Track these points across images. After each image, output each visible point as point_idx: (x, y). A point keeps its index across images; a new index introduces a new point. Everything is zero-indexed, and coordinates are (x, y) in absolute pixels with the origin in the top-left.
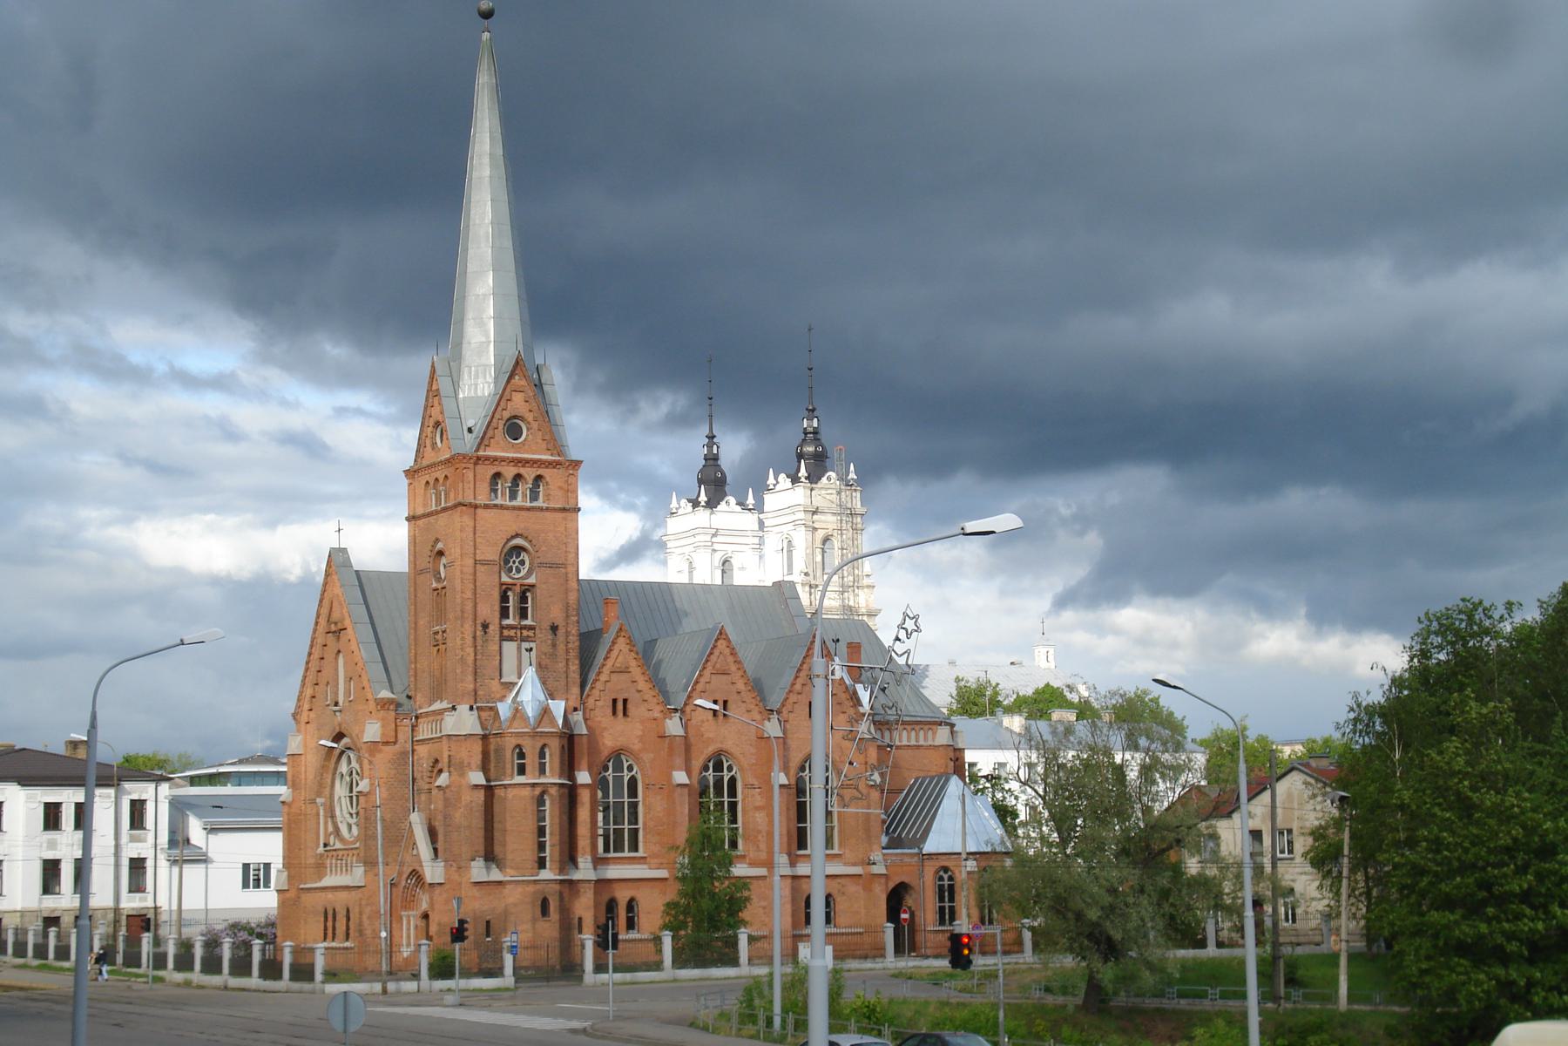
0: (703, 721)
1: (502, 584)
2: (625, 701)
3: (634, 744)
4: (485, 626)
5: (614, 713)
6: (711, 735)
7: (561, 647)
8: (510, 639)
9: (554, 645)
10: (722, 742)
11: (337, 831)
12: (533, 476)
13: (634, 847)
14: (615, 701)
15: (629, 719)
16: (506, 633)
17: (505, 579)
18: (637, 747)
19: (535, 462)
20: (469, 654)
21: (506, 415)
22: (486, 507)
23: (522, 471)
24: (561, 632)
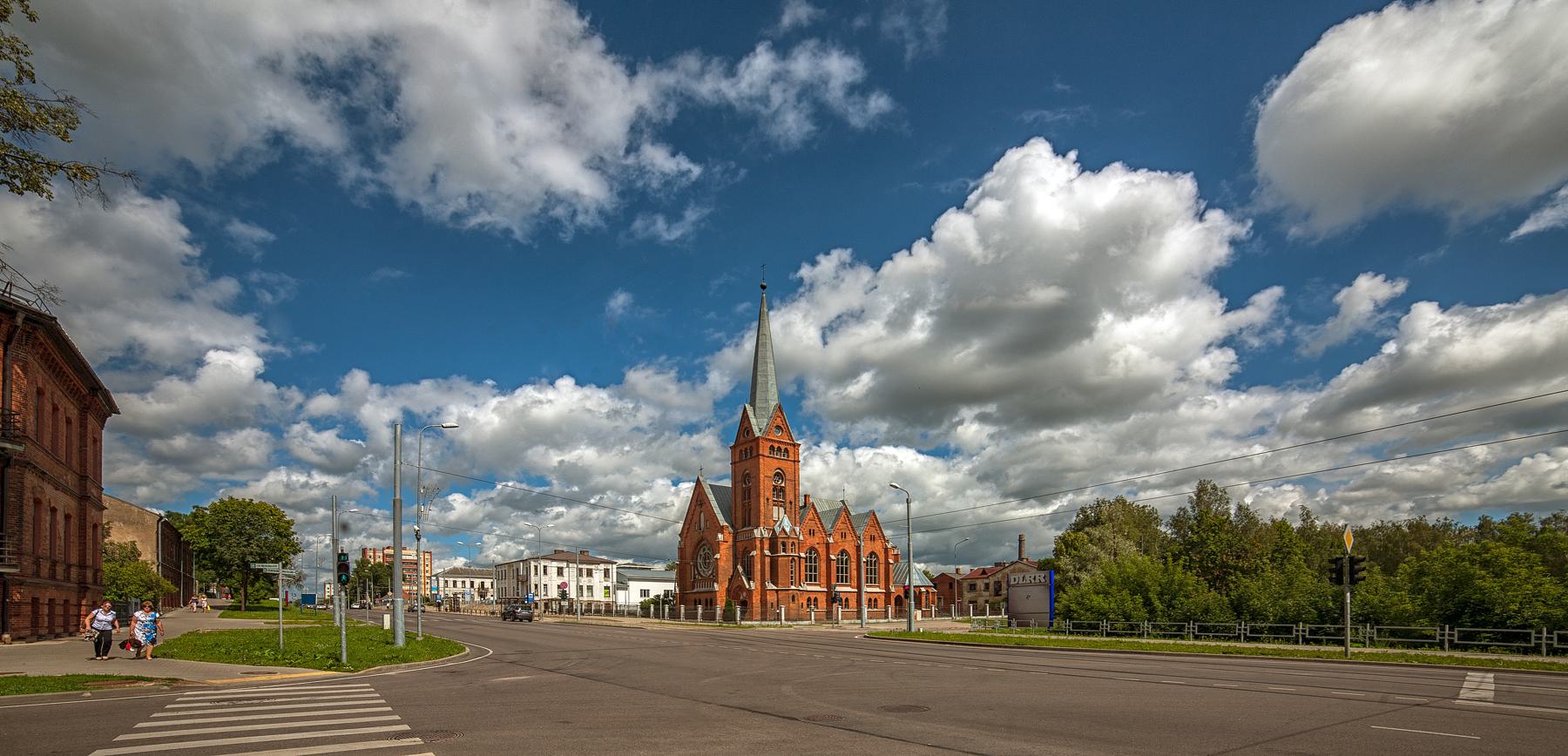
4: (768, 499)
11: (699, 574)
21: (775, 425)
22: (768, 457)
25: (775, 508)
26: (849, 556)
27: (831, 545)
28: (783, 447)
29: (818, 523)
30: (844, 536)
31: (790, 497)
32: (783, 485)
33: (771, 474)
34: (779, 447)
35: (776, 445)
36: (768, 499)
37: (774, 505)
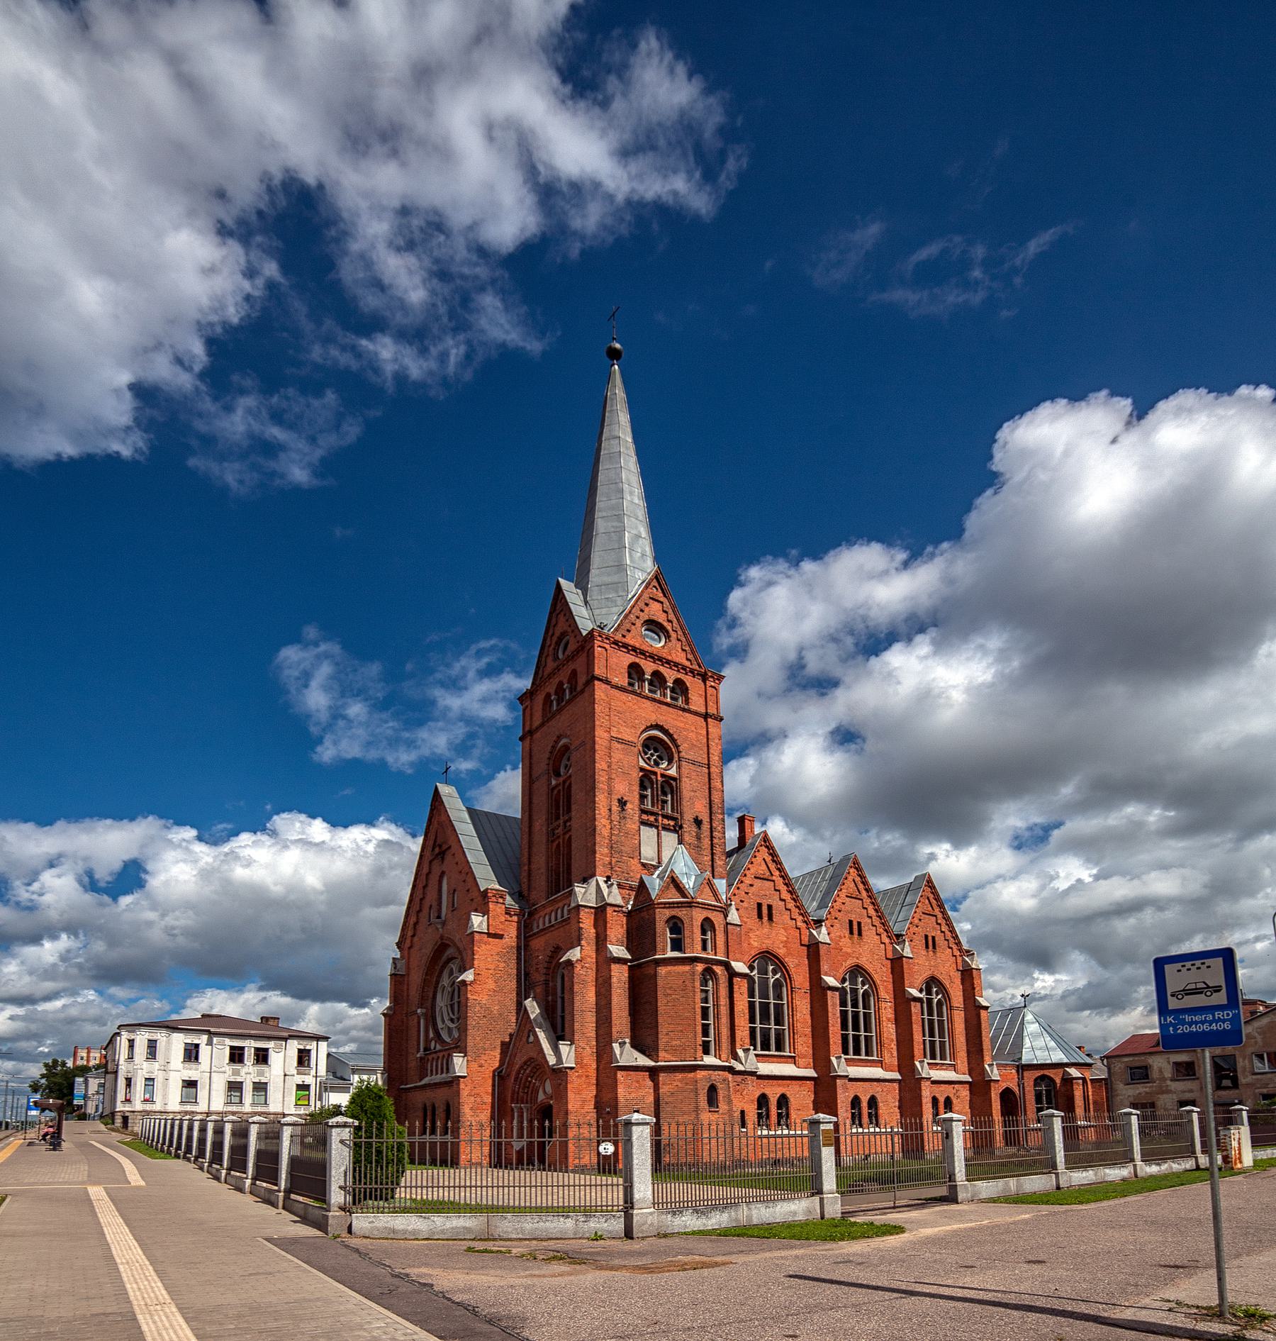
0: (840, 937)
1: (642, 769)
2: (770, 907)
3: (779, 948)
4: (622, 803)
5: (760, 916)
6: (849, 950)
7: (706, 842)
8: (650, 825)
9: (698, 838)
10: (857, 958)
12: (673, 678)
13: (779, 1048)
14: (759, 905)
15: (774, 924)
16: (645, 817)
17: (642, 763)
18: (781, 952)
19: (676, 664)
20: (605, 826)
23: (662, 669)
24: (706, 826)
25: (648, 834)
26: (874, 985)
27: (823, 949)
28: (670, 675)
29: (783, 888)
30: (855, 929)
31: (694, 805)
32: (673, 772)
33: (634, 735)
34: (656, 674)
35: (649, 667)
36: (622, 803)
37: (643, 823)
